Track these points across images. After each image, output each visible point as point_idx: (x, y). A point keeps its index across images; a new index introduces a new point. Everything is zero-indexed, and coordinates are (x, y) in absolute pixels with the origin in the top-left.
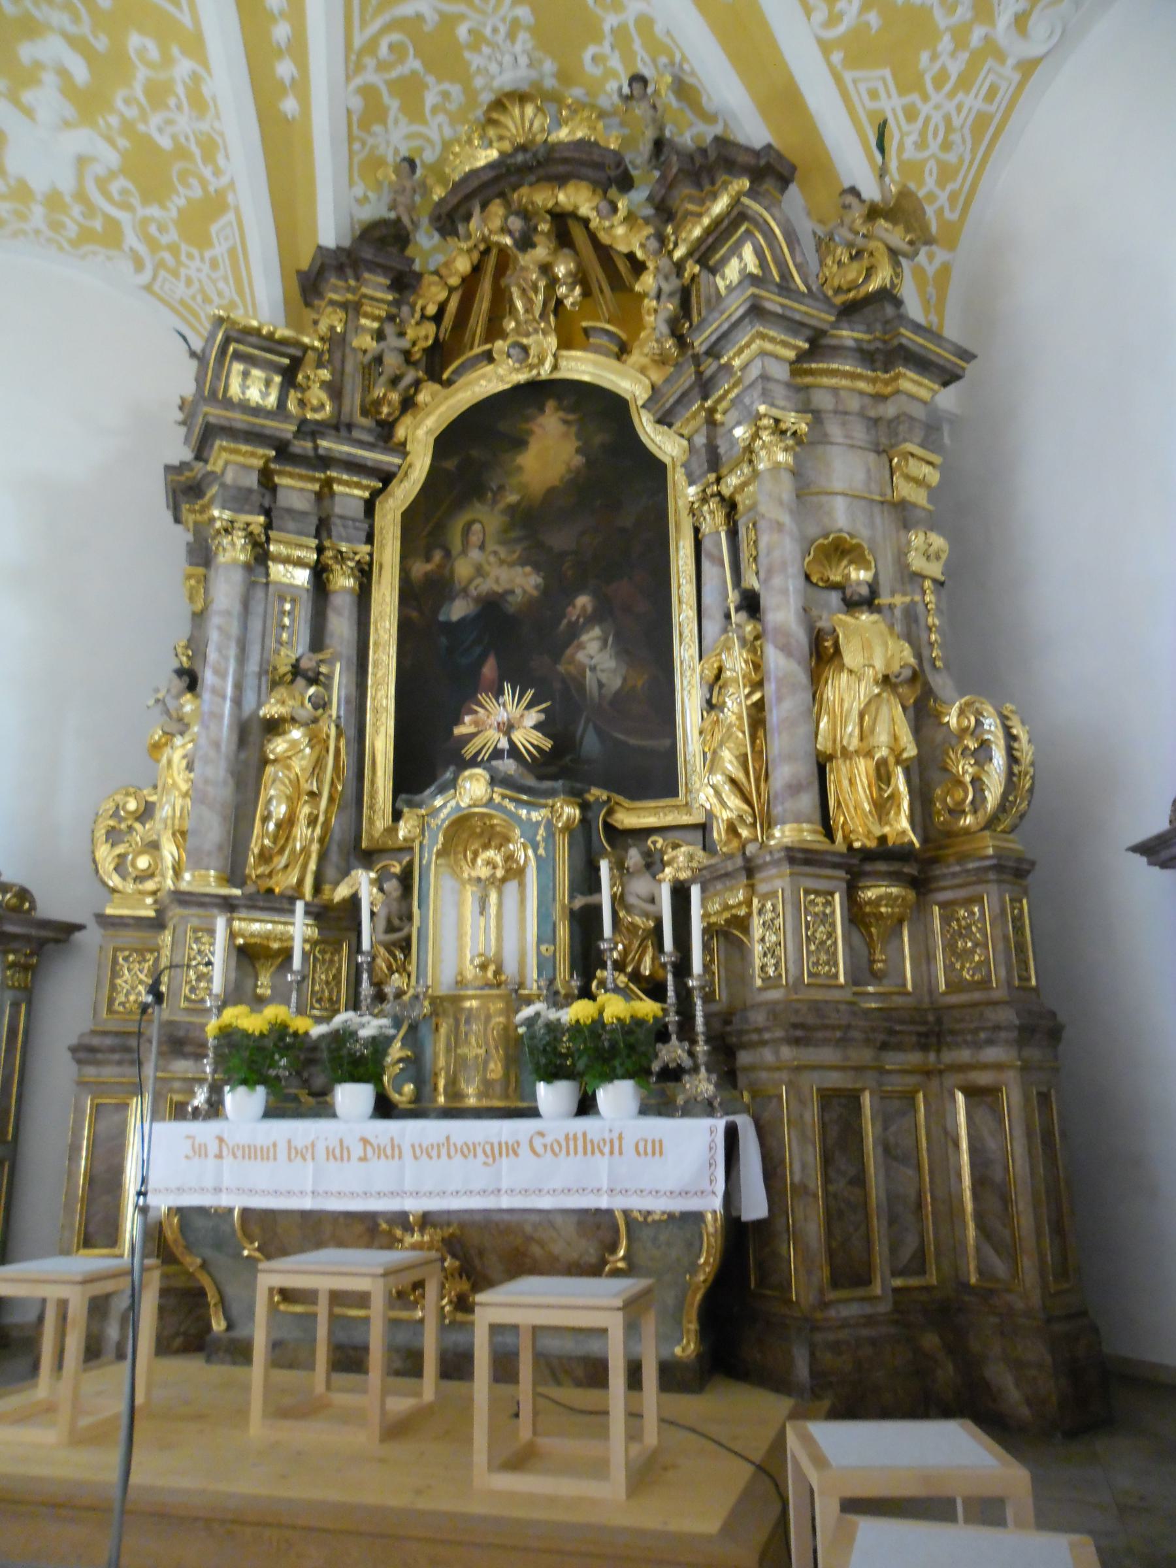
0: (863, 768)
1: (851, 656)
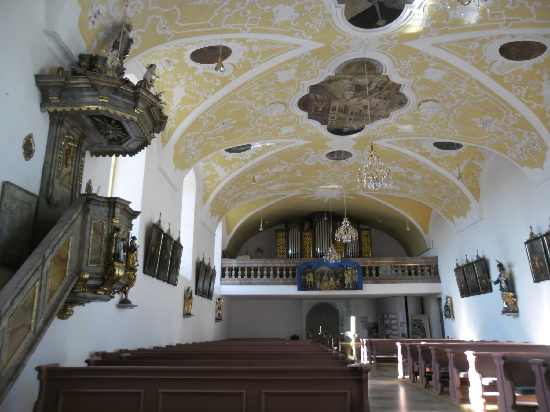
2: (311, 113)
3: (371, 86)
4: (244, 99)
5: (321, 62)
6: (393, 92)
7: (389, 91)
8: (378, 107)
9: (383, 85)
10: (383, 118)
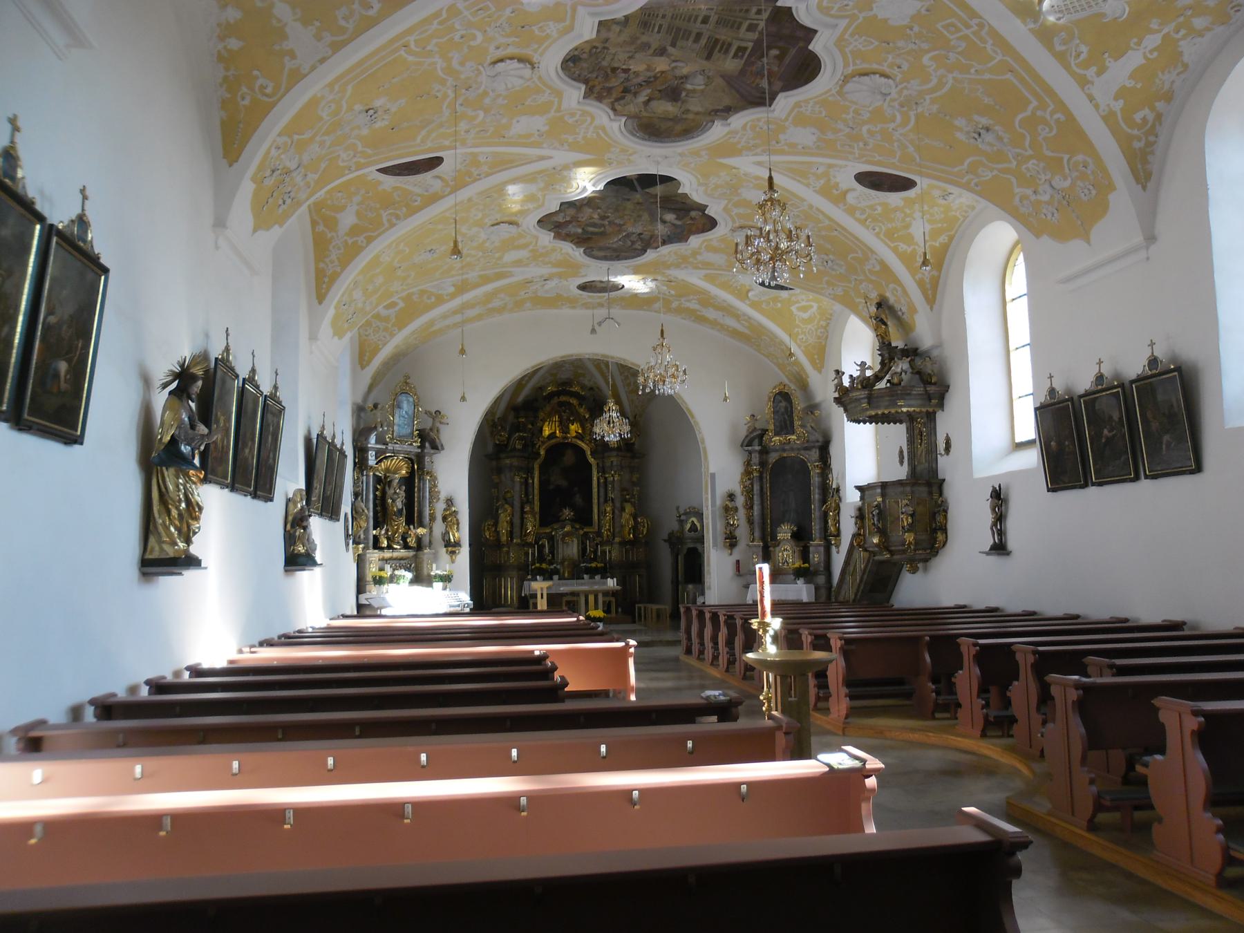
0: (627, 529)
1: (626, 511)
2: (801, 44)
3: (647, 96)
4: (896, 144)
5: (731, 140)
6: (599, 83)
7: (607, 85)
8: (629, 52)
9: (623, 98)
10: (614, 21)
